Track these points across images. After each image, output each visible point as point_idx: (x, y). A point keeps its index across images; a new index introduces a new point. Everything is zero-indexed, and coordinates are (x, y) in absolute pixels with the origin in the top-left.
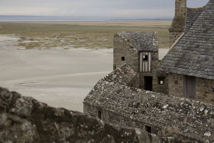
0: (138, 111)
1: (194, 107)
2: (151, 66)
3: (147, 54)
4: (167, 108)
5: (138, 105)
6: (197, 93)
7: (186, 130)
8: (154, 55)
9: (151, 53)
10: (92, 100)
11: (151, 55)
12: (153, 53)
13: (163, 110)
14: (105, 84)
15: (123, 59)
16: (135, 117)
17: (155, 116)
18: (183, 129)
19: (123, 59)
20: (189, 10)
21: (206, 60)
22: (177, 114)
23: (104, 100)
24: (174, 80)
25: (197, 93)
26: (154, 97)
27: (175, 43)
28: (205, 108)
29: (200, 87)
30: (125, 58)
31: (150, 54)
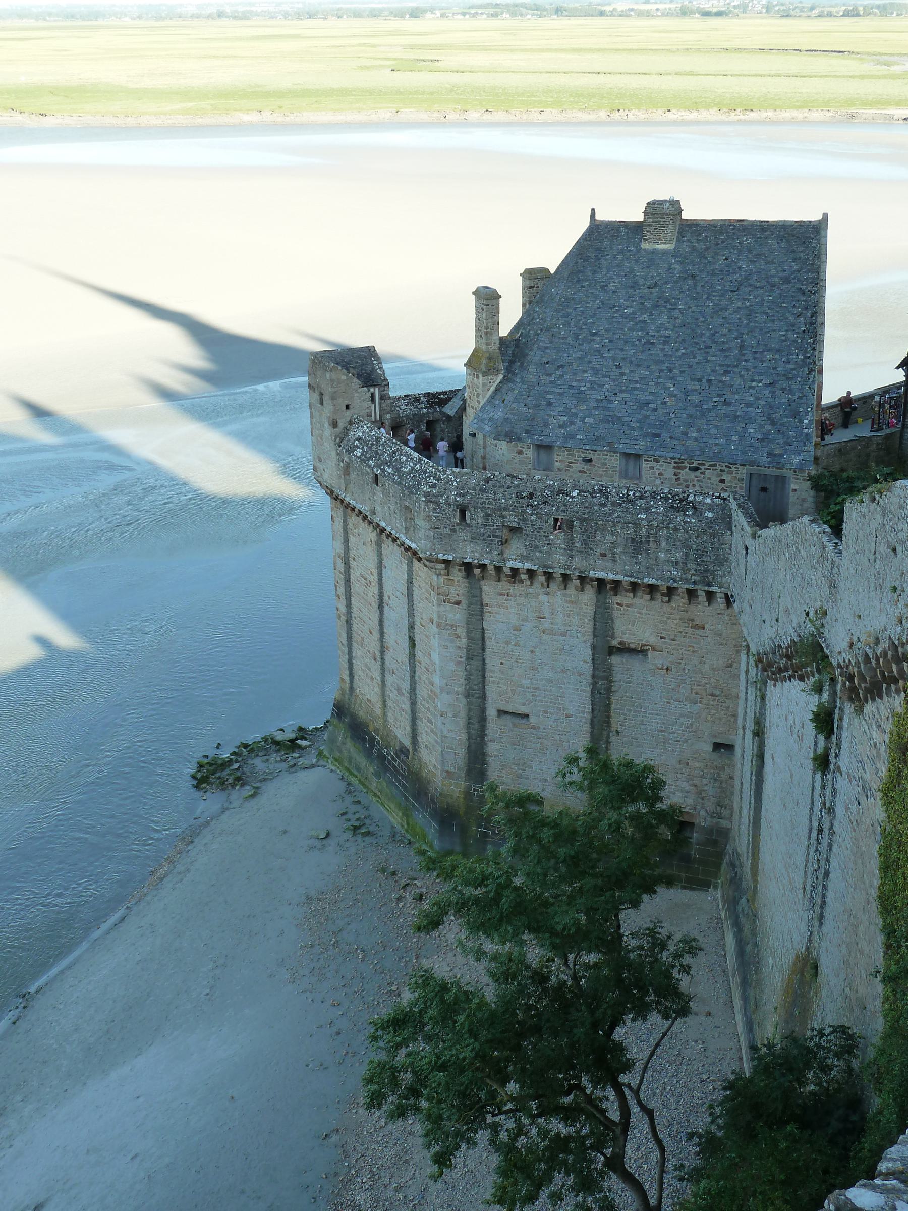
0: (536, 503)
1: (614, 491)
2: (380, 411)
3: (372, 390)
4: (579, 494)
5: (531, 496)
6: (556, 464)
7: (616, 515)
8: (384, 390)
9: (379, 389)
10: (442, 496)
11: (379, 391)
12: (382, 389)
13: (572, 497)
14: (453, 472)
16: (535, 510)
17: (565, 505)
19: (347, 407)
20: (501, 338)
21: (572, 423)
22: (595, 500)
23: (467, 493)
24: (515, 449)
25: (556, 464)
26: (552, 483)
27: (490, 392)
30: (351, 407)
31: (377, 389)
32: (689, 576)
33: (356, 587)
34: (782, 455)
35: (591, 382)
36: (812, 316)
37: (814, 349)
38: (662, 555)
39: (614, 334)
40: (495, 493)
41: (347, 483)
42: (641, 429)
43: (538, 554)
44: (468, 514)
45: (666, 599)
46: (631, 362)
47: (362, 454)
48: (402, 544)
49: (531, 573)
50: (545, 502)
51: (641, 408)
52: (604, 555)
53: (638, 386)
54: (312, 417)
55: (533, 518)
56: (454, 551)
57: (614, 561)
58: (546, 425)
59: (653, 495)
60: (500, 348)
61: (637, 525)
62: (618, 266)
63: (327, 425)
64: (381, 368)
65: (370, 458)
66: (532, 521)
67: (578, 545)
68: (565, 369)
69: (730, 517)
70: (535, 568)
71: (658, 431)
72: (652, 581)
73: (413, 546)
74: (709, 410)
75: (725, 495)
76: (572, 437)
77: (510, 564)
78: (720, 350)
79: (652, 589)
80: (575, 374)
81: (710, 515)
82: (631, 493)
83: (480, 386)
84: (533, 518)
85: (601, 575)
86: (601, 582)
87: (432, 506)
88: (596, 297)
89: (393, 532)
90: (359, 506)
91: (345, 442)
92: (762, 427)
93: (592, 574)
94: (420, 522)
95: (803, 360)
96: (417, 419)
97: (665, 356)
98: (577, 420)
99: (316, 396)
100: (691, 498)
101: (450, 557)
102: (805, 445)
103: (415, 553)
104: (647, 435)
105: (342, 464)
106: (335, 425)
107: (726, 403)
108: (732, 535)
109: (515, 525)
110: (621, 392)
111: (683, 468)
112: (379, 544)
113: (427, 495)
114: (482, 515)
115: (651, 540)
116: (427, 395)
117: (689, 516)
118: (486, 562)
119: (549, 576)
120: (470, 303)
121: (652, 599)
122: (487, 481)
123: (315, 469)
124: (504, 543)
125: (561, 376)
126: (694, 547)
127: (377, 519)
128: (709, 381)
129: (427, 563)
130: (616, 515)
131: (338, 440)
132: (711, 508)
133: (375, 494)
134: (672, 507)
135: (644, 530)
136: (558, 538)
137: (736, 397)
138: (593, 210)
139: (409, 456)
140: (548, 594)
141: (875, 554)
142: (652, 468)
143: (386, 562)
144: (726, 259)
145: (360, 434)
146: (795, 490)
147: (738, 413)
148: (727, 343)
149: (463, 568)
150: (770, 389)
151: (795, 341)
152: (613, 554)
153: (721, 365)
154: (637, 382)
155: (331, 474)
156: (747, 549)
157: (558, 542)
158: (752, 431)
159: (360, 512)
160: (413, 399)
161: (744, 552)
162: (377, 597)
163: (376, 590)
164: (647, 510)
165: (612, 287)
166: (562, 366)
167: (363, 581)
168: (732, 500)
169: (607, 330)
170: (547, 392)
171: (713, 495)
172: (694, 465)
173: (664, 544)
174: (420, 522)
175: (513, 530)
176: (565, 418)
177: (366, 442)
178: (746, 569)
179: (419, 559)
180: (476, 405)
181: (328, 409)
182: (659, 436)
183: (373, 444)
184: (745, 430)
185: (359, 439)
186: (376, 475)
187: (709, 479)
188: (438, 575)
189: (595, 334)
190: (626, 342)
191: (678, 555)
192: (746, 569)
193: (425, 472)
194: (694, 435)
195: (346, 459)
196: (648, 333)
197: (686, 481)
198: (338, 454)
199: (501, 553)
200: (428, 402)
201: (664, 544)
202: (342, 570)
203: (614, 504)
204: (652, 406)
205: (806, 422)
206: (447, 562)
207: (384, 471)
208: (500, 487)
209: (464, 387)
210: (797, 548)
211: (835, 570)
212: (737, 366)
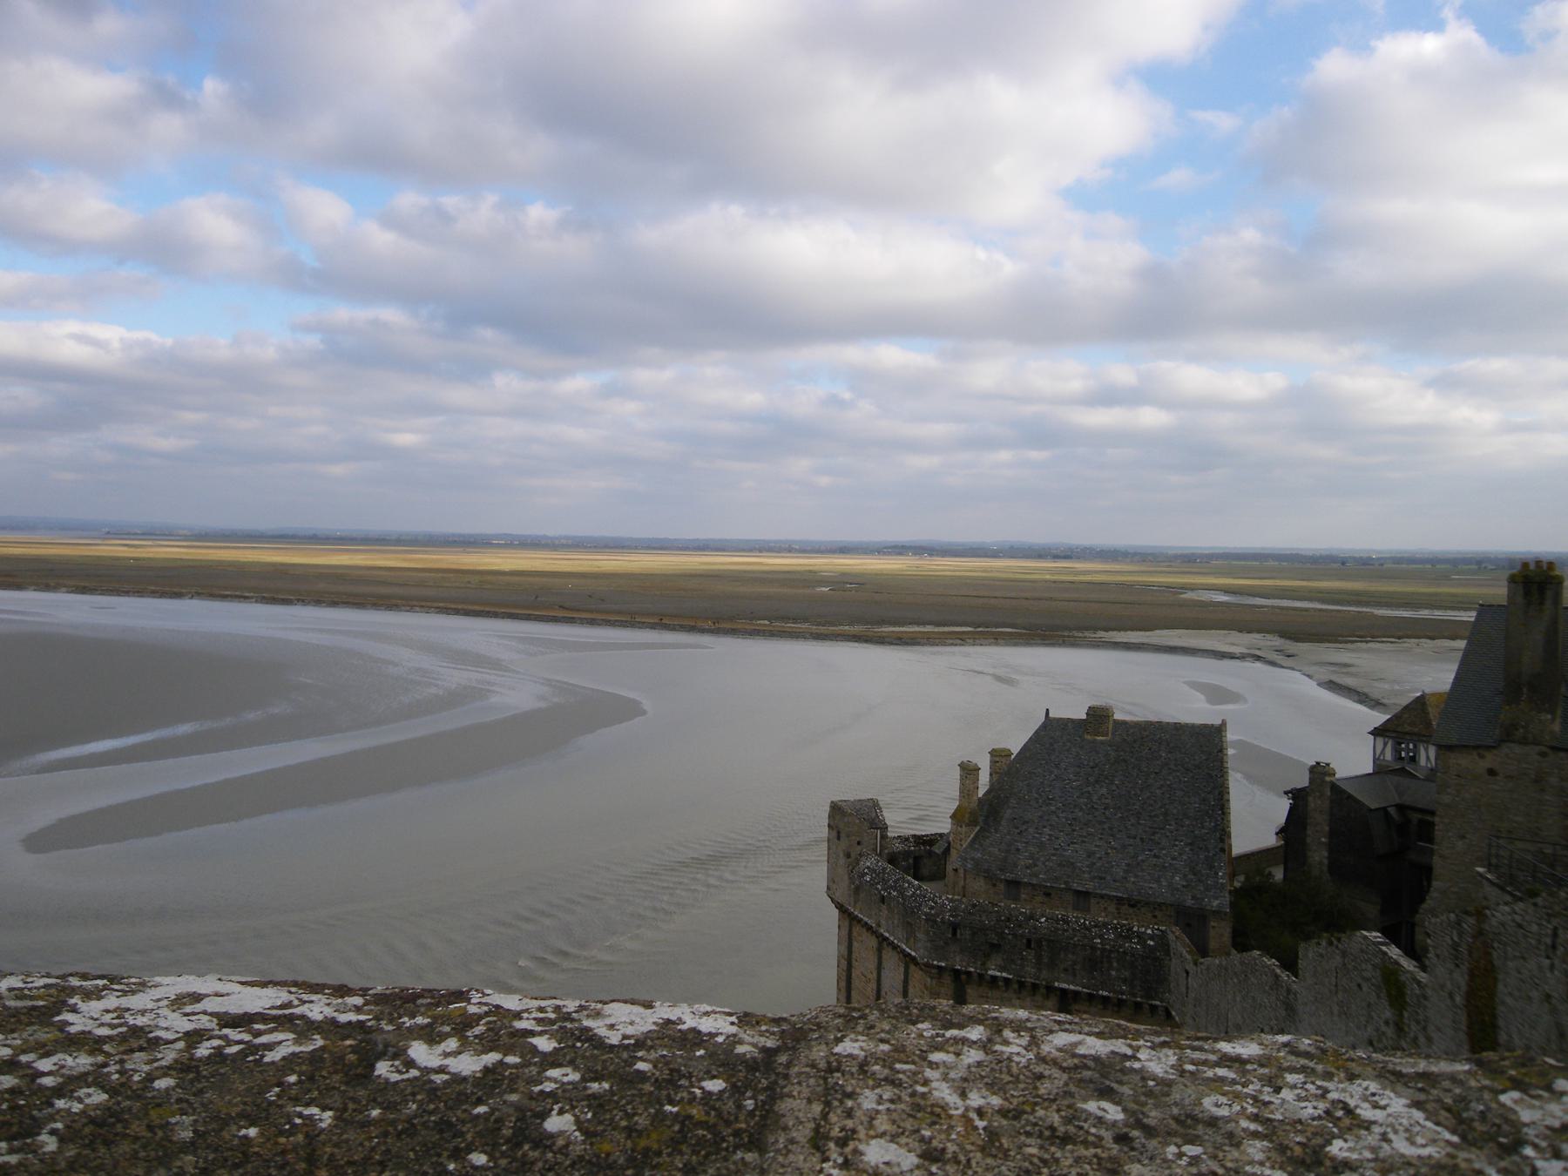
5: (1008, 920)
6: (1023, 896)
7: (1076, 939)
13: (1041, 923)
15: (859, 843)
17: (1035, 928)
18: (1072, 939)
19: (859, 843)
21: (1036, 865)
25: (1023, 896)
27: (970, 838)
28: (1085, 920)
29: (1026, 891)
32: (1136, 991)
33: (856, 983)
34: (1203, 899)
35: (1050, 835)
36: (1219, 794)
37: (1223, 819)
38: (1113, 973)
39: (1066, 800)
40: (980, 917)
41: (855, 903)
42: (1090, 873)
43: (1013, 966)
44: (958, 931)
45: (1116, 1009)
46: (1080, 822)
47: (871, 879)
48: (903, 951)
49: (1006, 980)
50: (1020, 926)
51: (1089, 857)
52: (1066, 970)
53: (1086, 840)
54: (829, 849)
55: (1010, 937)
56: (947, 960)
57: (1074, 975)
58: (1015, 865)
59: (1105, 925)
60: (978, 806)
61: (1093, 948)
62: (1068, 750)
63: (841, 855)
64: (882, 815)
65: (878, 883)
66: (1009, 940)
67: (1046, 960)
68: (1029, 825)
69: (1168, 945)
70: (1011, 977)
71: (1104, 875)
72: (1105, 993)
73: (913, 954)
74: (1143, 861)
75: (1164, 928)
76: (1036, 875)
77: (990, 972)
78: (1150, 816)
79: (1105, 1000)
80: (1037, 828)
81: (1152, 943)
82: (1087, 922)
83: (963, 833)
84: (1010, 937)
85: (1065, 986)
86: (1064, 991)
87: (930, 923)
88: (1051, 772)
89: (896, 941)
90: (866, 919)
91: (857, 869)
92: (1185, 876)
93: (1056, 984)
94: (920, 935)
95: (1215, 827)
96: (907, 854)
97: (1107, 818)
98: (1040, 864)
99: (834, 833)
100: (1136, 929)
101: (943, 964)
102: (1221, 892)
103: (913, 959)
104: (1095, 877)
105: (853, 886)
106: (848, 856)
107: (1155, 856)
108: (1170, 960)
109: (995, 942)
110: (1072, 843)
111: (1124, 904)
112: (880, 950)
113: (926, 914)
114: (970, 932)
115: (1105, 960)
116: (914, 836)
117: (1134, 943)
118: (972, 970)
119: (1022, 985)
120: (957, 773)
121: (1105, 1008)
122: (974, 906)
123: (828, 888)
124: (987, 956)
125: (1026, 830)
126: (1140, 968)
127: (882, 931)
128: (1142, 839)
129: (923, 967)
130: (1076, 939)
131: (851, 868)
132: (1152, 937)
133: (880, 911)
134: (1121, 935)
135: (1099, 952)
136: (1030, 955)
137: (1164, 852)
138: (1047, 710)
139: (909, 883)
140: (1019, 998)
141: (1336, 986)
142: (1098, 903)
143: (885, 964)
144: (1150, 749)
145: (869, 864)
146: (1214, 927)
147: (1167, 865)
148: (1153, 811)
149: (952, 973)
150: (1190, 847)
151: (1208, 813)
152: (1074, 969)
153: (1150, 828)
154: (1085, 837)
155: (843, 893)
156: (1187, 973)
157: (1030, 957)
158: (1178, 878)
159: (866, 923)
160: (904, 839)
161: (1185, 975)
162: (874, 992)
163: (875, 987)
164: (1101, 937)
165: (1063, 765)
166: (1028, 822)
167: (864, 979)
168: (1168, 932)
169: (1060, 797)
170: (1016, 841)
171: (1153, 927)
172: (1132, 903)
173: (1115, 964)
174: (920, 935)
175: (993, 946)
176: (1031, 861)
177: (874, 871)
178: (1187, 988)
179: (916, 964)
180: (959, 847)
181: (844, 843)
182: (1104, 879)
183: (880, 873)
184: (1173, 877)
185: (868, 868)
186: (883, 896)
187: (1144, 914)
188: (932, 978)
189: (1052, 799)
190: (1075, 806)
191: (1127, 973)
192: (1187, 988)
193: (925, 897)
194: (1132, 879)
195: (857, 882)
196: (1092, 801)
197: (1126, 914)
198: (850, 878)
199: (983, 964)
200: (915, 842)
201: (1115, 964)
202: (845, 969)
203: (1074, 929)
204: (1098, 855)
205: (1220, 874)
206: (939, 968)
207: (890, 893)
208: (984, 912)
209: (949, 834)
210: (1246, 976)
211: (1291, 997)
212: (1163, 829)
